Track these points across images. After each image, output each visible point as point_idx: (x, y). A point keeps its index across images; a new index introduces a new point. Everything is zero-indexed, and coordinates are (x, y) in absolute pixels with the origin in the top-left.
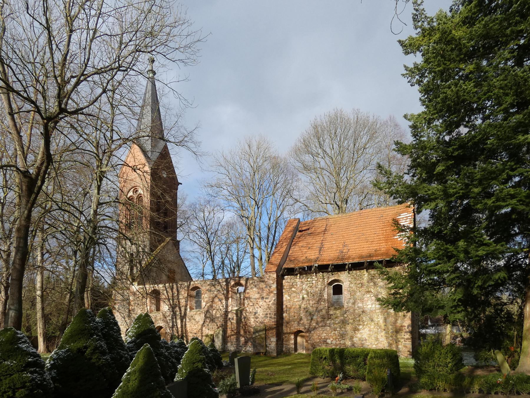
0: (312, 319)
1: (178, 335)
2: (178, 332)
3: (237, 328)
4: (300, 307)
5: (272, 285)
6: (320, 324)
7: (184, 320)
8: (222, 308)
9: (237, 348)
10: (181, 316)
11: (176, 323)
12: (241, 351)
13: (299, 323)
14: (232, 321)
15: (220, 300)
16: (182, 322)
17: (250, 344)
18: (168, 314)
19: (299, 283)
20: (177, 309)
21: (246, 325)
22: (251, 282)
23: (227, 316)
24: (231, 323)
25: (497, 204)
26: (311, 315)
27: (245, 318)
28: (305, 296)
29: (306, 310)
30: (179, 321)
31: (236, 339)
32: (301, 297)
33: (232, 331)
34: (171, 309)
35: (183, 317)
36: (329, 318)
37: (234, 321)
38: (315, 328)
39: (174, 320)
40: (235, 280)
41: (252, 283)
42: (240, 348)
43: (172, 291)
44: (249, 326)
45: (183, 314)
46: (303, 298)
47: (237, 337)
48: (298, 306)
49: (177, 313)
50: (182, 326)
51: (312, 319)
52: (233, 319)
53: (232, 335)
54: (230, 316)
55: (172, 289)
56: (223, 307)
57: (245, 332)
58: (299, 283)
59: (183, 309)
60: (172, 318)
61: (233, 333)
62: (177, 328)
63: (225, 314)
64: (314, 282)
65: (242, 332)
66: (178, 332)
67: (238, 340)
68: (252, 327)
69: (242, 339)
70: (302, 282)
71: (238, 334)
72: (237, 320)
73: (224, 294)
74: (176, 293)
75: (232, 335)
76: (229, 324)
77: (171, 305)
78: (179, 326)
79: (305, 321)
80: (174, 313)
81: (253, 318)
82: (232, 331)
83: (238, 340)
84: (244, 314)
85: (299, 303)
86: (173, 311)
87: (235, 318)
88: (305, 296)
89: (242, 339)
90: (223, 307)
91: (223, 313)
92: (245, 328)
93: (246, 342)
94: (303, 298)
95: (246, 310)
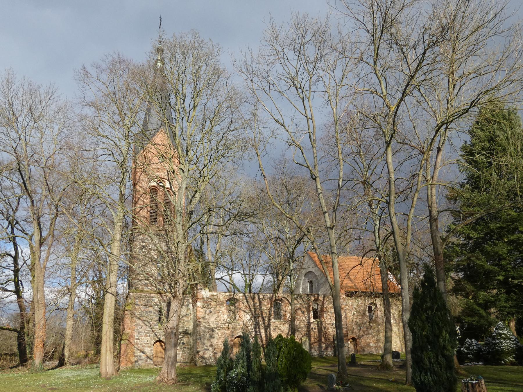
0: (360, 329)
1: (263, 345)
2: (262, 342)
3: (319, 336)
4: (352, 321)
5: (343, 303)
6: (366, 333)
7: (268, 330)
8: (305, 319)
9: (320, 353)
10: (265, 326)
11: (260, 332)
12: (323, 355)
13: (352, 332)
14: (315, 331)
15: (303, 313)
16: (266, 331)
17: (329, 349)
18: (249, 323)
19: (350, 303)
20: (260, 319)
21: (326, 333)
22: (327, 299)
23: (310, 326)
24: (314, 332)
25: (301, 287)
26: (359, 326)
27: (325, 328)
28: (355, 313)
29: (356, 322)
30: (263, 331)
31: (319, 346)
32: (353, 313)
33: (316, 339)
34: (253, 319)
35: (267, 326)
36: (370, 329)
37: (316, 330)
38: (362, 336)
39: (258, 330)
40: (314, 297)
41: (328, 301)
42: (323, 353)
43: (254, 301)
44: (329, 335)
45: (266, 324)
46: (354, 314)
47: (319, 344)
48: (351, 320)
49: (261, 323)
50: (266, 335)
51: (360, 329)
52: (315, 329)
53: (316, 342)
54: (312, 326)
55: (253, 299)
56: (306, 318)
57: (326, 339)
58: (350, 303)
59: (266, 319)
60: (255, 328)
61: (316, 341)
62: (261, 337)
63: (308, 324)
64: (360, 303)
65: (323, 340)
66: (262, 342)
67: (320, 346)
68: (331, 336)
69: (324, 345)
70: (353, 303)
71: (320, 341)
72: (318, 329)
73: (305, 307)
74: (258, 303)
75: (316, 342)
76: (312, 333)
77: (252, 314)
78: (263, 335)
79: (356, 330)
80: (256, 323)
81: (331, 328)
82: (316, 339)
83: (320, 346)
84: (324, 325)
85: (352, 317)
86: (255, 321)
87: (316, 327)
88: (355, 313)
89: (324, 345)
90: (306, 318)
91: (306, 323)
92: (326, 336)
93: (327, 348)
94: (354, 314)
95: (325, 322)
